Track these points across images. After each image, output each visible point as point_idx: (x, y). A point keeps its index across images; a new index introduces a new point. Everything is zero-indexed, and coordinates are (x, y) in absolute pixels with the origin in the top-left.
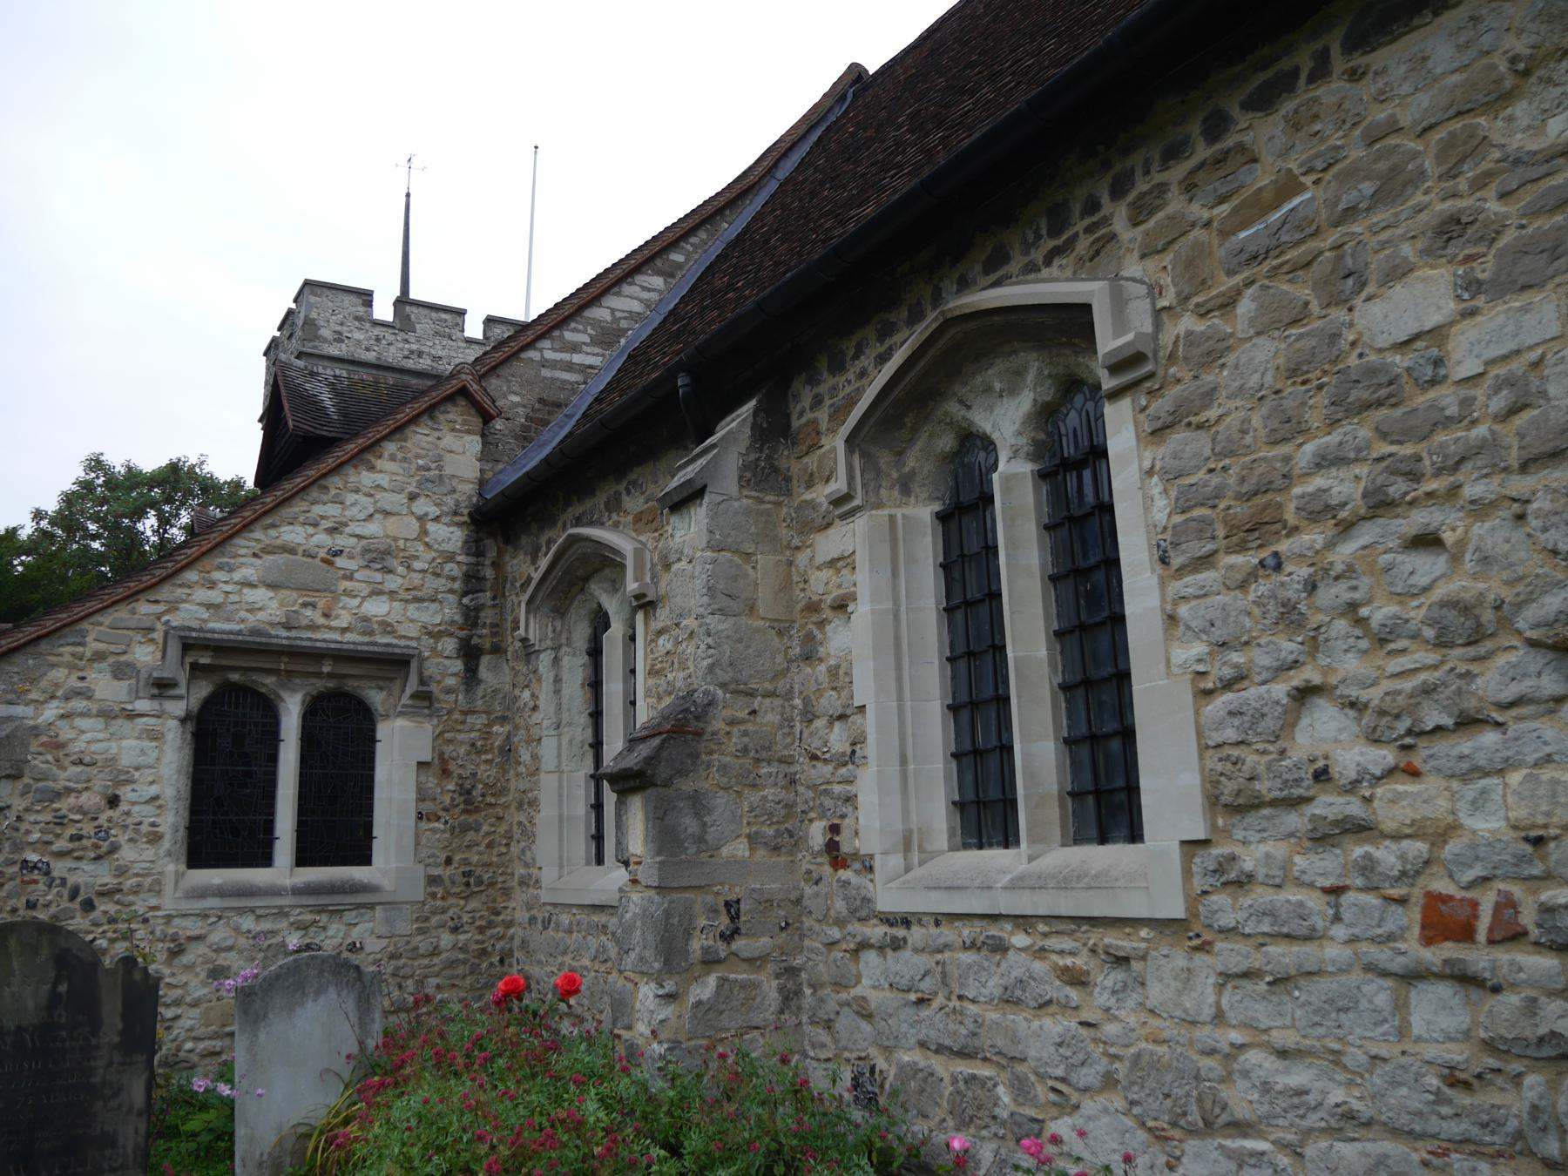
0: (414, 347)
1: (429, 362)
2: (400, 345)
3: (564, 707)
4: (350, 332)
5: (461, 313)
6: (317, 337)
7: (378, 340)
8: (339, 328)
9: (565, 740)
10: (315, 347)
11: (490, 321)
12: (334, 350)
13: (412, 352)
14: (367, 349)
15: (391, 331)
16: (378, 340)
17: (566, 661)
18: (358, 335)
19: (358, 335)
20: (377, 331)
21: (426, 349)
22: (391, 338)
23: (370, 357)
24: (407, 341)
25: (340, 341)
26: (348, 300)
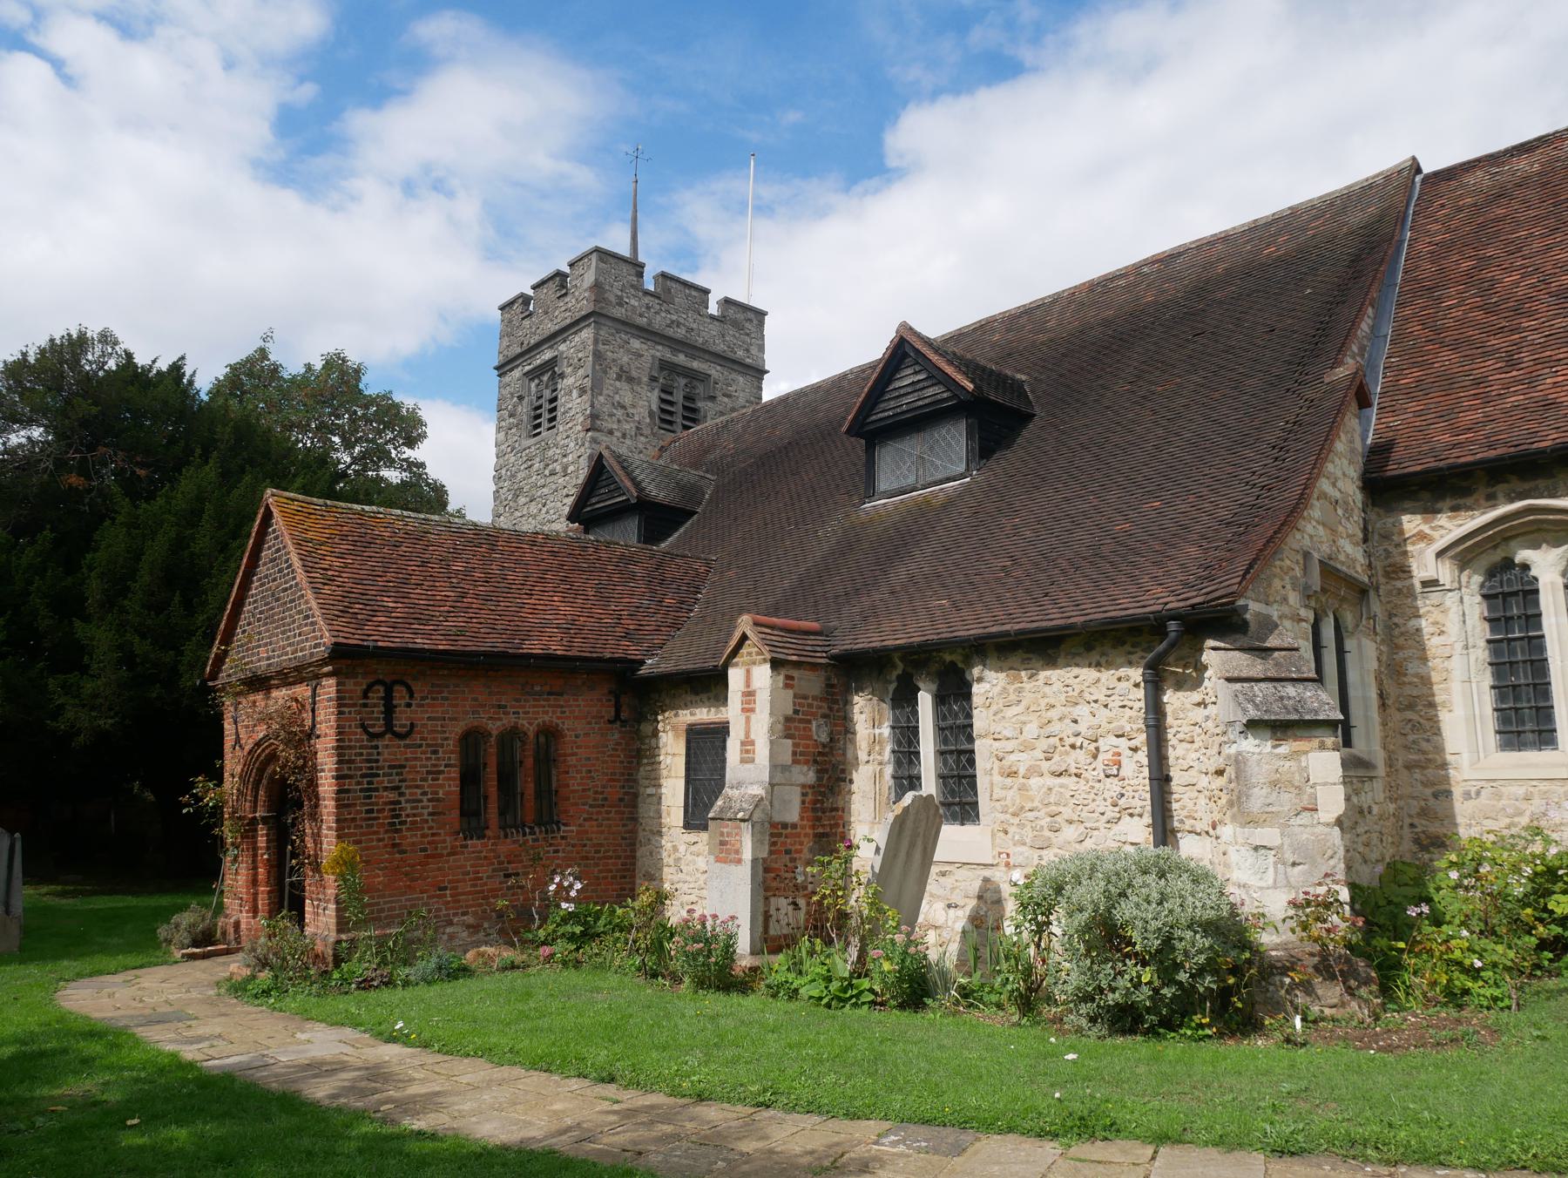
0: (674, 318)
1: (684, 332)
2: (663, 314)
3: (1469, 633)
4: (627, 297)
5: (706, 292)
6: (608, 302)
7: (648, 308)
8: (620, 293)
9: (1472, 659)
10: (602, 308)
11: (727, 302)
12: (618, 312)
13: (673, 322)
14: (641, 315)
15: (657, 301)
16: (648, 308)
17: (1466, 598)
18: (634, 302)
19: (634, 302)
20: (647, 299)
21: (682, 321)
22: (658, 307)
23: (643, 321)
24: (668, 312)
25: (620, 304)
26: (625, 268)
